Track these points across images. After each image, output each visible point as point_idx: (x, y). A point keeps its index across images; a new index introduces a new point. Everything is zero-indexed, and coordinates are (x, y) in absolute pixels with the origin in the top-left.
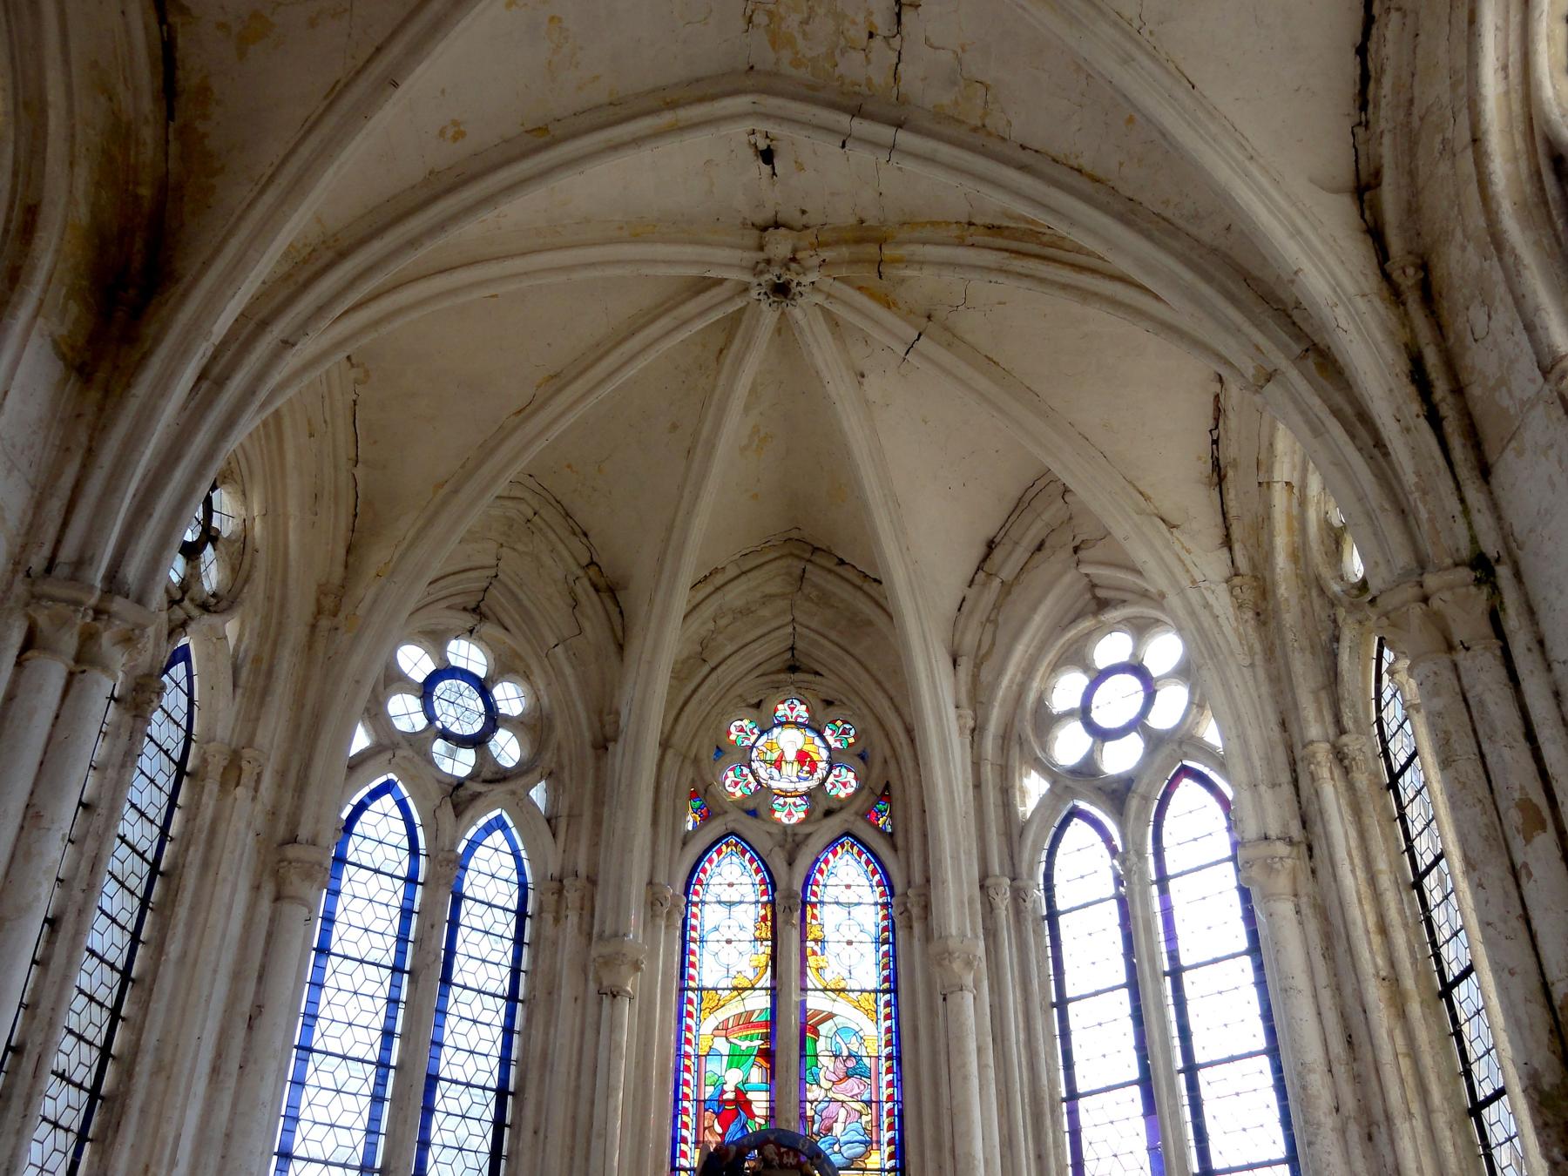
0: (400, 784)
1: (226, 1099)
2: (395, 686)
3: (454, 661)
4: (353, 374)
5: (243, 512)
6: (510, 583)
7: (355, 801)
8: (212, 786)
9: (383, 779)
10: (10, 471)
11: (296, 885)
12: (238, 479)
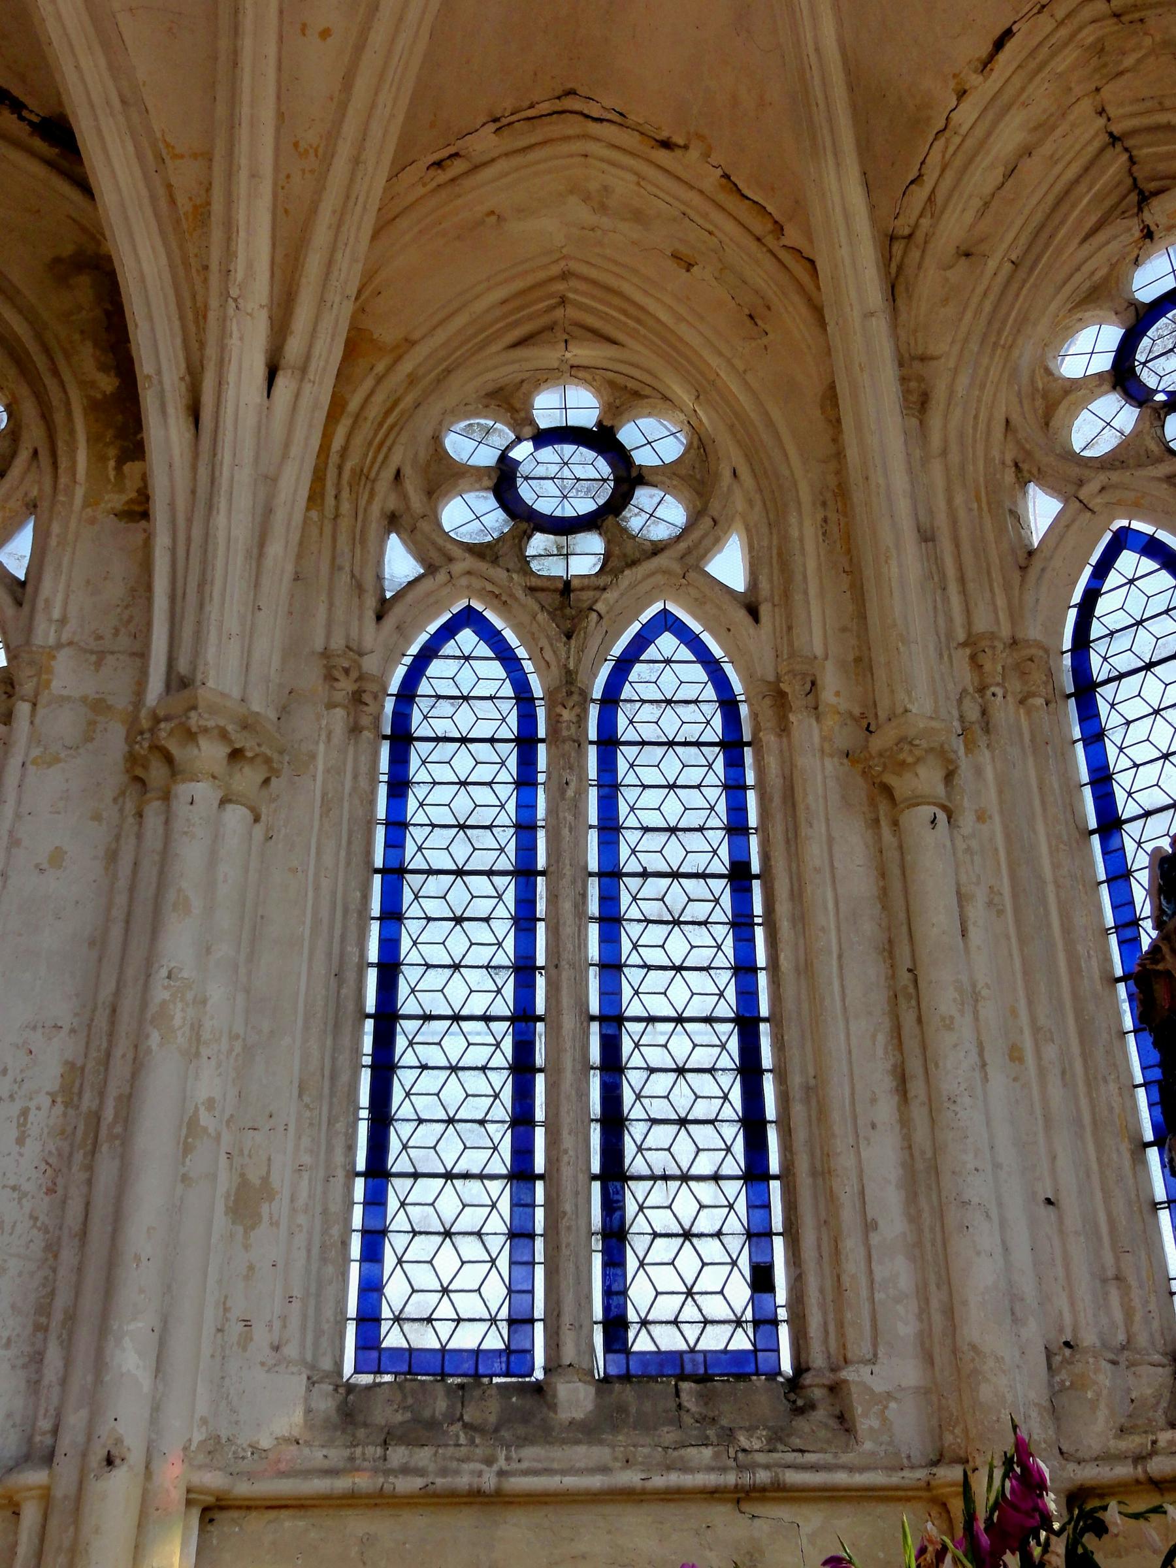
0: (1136, 525)
1: (919, 1114)
2: (1061, 410)
3: (1146, 295)
4: (694, 154)
5: (682, 417)
6: (1147, 121)
7: (1077, 597)
8: (769, 739)
9: (1108, 536)
10: (98, 664)
11: (902, 785)
12: (647, 391)
